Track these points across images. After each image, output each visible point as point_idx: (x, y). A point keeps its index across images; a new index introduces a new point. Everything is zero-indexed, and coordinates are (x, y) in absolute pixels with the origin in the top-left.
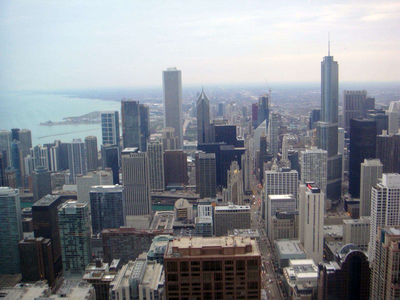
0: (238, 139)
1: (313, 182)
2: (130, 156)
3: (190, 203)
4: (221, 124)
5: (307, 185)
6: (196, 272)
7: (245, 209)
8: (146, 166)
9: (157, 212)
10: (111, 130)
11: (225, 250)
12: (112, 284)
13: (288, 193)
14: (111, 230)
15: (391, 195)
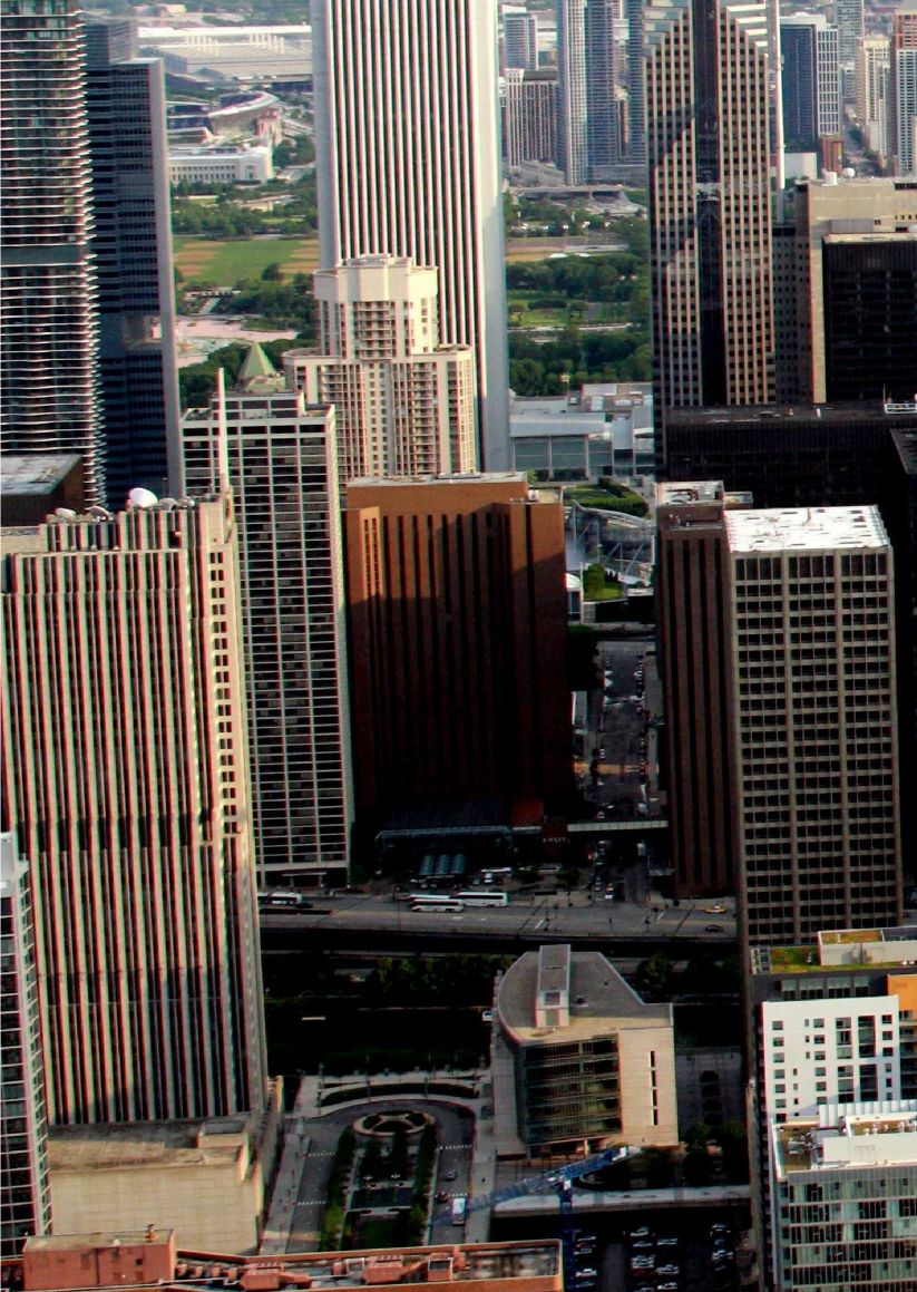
2: (54, 545)
3: (635, 980)
8: (211, 637)
9: (311, 1087)
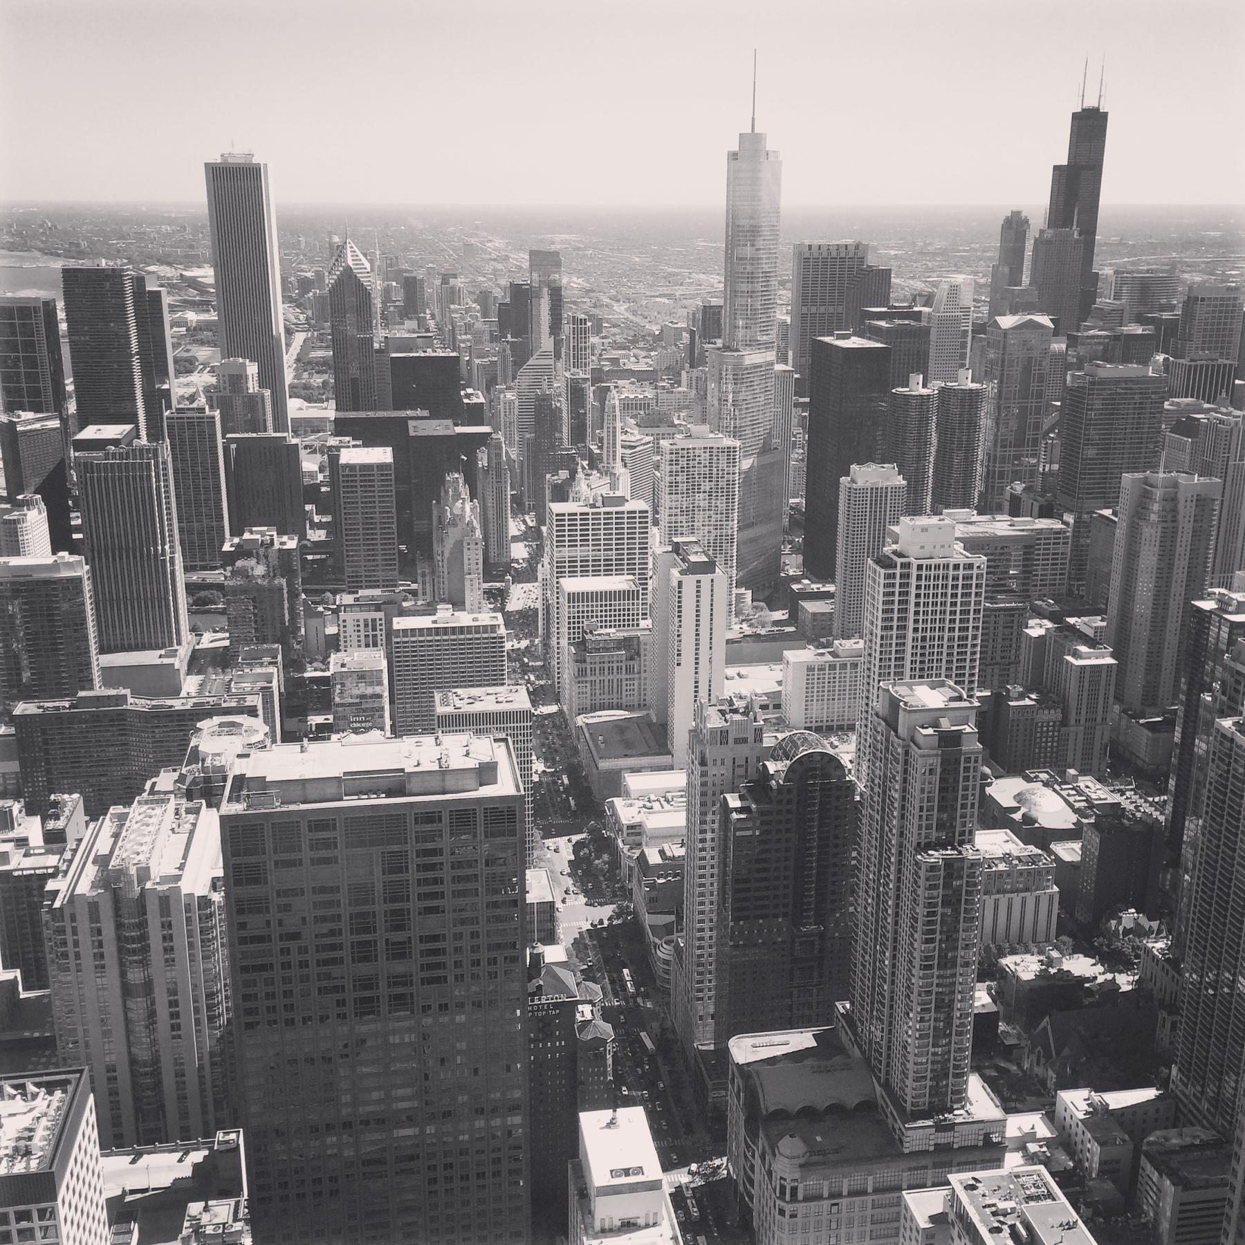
0: (466, 401)
1: (694, 539)
4: (411, 351)
5: (677, 548)
6: (324, 853)
7: (488, 622)
10: (32, 363)
11: (414, 780)
12: (51, 885)
13: (619, 572)
14: (46, 705)
15: (923, 583)
